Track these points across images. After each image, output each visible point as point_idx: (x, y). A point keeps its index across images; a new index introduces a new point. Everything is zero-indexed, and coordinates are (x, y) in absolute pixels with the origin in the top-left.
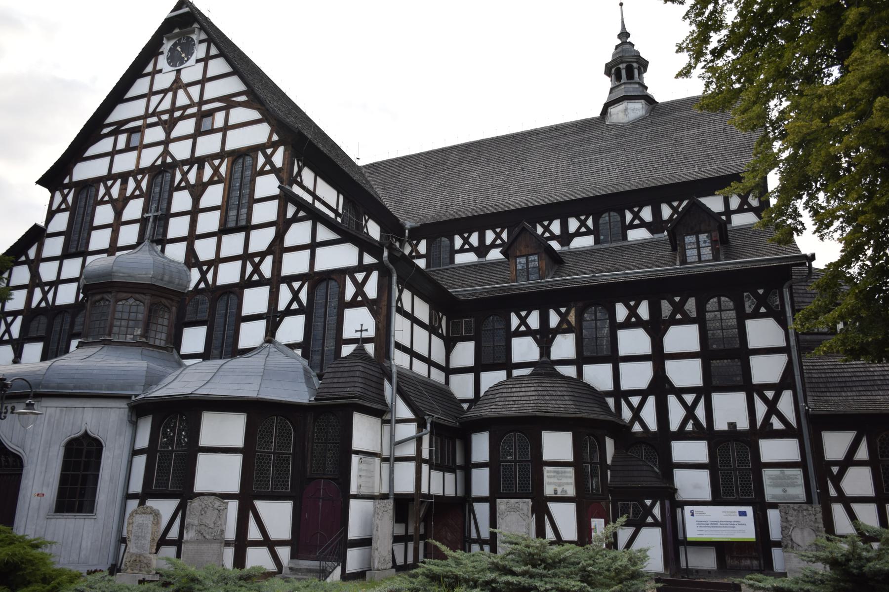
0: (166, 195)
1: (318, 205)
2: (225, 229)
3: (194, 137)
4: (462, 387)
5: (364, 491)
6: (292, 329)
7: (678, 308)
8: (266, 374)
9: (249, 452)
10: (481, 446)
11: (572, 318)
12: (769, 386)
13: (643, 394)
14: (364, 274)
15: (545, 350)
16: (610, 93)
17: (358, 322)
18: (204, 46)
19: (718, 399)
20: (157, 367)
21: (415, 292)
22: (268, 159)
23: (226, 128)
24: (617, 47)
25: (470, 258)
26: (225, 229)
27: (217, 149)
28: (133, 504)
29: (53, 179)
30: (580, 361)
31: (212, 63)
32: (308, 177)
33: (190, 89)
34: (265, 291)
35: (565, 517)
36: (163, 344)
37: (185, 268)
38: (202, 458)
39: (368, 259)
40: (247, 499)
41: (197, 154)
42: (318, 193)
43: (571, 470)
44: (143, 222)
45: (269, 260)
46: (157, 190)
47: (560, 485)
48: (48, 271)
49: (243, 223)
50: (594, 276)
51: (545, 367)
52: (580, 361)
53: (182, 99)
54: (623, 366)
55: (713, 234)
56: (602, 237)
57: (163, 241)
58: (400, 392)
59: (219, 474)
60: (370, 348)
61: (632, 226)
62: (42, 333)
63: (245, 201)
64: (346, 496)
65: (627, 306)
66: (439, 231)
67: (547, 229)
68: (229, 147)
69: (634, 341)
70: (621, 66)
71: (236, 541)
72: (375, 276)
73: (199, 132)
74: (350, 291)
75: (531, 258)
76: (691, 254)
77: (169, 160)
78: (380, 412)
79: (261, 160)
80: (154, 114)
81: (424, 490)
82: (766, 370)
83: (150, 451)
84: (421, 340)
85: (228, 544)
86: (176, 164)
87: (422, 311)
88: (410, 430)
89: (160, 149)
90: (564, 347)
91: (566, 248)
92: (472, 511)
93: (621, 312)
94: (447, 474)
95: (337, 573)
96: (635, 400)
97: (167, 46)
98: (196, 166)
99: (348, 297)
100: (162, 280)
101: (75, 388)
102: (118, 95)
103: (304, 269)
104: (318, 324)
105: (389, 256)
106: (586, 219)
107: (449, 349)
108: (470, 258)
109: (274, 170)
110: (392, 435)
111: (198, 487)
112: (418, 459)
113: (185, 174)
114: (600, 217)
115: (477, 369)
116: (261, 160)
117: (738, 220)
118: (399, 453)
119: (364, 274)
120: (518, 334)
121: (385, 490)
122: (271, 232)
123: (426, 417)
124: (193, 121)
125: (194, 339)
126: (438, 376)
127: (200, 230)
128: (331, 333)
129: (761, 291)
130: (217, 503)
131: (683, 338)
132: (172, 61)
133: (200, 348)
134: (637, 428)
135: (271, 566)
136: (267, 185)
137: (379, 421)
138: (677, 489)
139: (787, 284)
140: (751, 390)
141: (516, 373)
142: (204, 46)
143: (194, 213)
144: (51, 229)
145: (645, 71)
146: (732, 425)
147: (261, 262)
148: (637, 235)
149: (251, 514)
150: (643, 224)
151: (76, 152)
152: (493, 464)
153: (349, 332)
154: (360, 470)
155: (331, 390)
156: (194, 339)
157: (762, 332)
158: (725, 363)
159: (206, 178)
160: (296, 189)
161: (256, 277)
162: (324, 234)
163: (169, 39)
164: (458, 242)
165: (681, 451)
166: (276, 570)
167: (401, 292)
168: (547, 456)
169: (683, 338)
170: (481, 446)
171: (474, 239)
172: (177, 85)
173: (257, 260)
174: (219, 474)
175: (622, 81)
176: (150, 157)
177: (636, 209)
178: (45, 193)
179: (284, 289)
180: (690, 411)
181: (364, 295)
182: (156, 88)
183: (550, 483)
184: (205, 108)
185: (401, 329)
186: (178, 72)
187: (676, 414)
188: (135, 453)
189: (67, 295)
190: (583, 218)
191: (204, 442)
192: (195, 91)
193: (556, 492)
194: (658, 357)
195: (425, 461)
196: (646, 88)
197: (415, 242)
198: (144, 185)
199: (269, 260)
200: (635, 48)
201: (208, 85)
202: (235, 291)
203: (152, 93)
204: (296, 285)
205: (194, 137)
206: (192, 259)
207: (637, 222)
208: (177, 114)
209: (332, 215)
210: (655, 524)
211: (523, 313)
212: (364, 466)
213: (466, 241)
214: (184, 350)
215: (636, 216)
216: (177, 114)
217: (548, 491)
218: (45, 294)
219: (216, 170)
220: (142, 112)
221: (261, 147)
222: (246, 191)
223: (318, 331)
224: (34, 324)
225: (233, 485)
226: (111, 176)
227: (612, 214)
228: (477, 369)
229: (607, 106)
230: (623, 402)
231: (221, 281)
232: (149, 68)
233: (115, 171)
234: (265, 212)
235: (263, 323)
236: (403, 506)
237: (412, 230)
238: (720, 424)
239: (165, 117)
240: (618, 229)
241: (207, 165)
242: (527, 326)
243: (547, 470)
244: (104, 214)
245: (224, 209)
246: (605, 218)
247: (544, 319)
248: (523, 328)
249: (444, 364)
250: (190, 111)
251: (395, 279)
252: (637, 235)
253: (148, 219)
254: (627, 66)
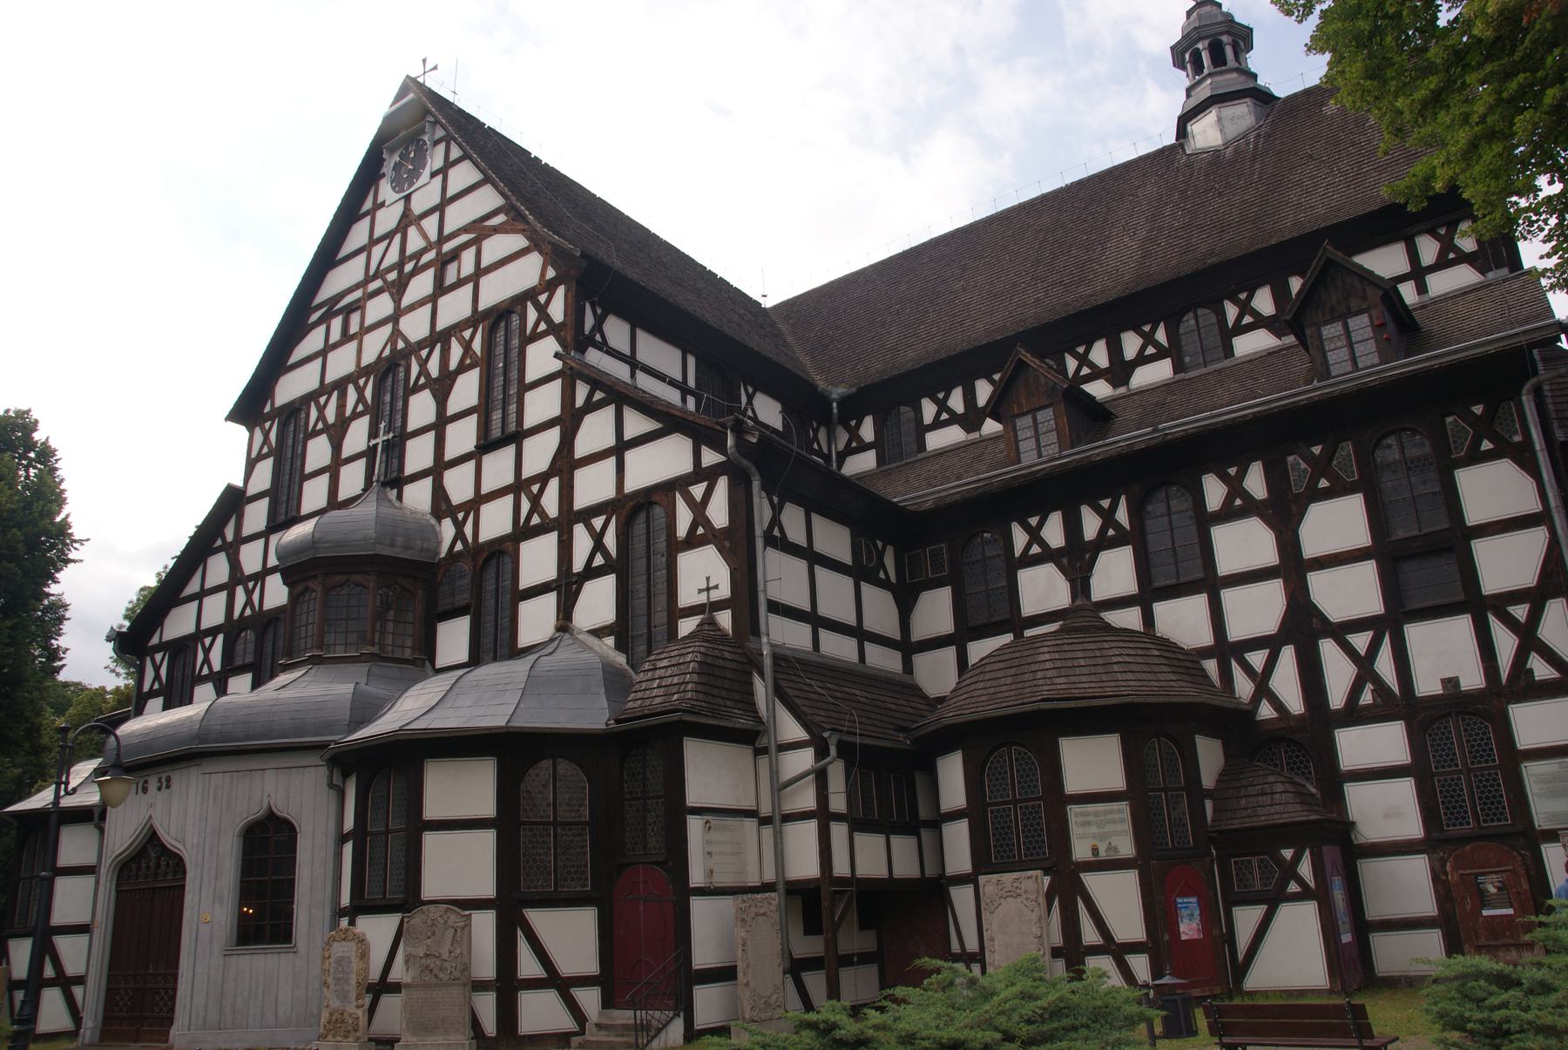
0: (400, 403)
1: (645, 382)
2: (487, 445)
3: (433, 299)
4: (937, 673)
5: (723, 879)
6: (598, 602)
7: (1321, 467)
8: (533, 683)
9: (508, 823)
10: (952, 777)
11: (1122, 515)
12: (1515, 596)
13: (1271, 644)
14: (705, 484)
15: (1080, 585)
16: (1188, 96)
17: (702, 574)
18: (441, 148)
19: (1418, 635)
20: (376, 690)
21: (813, 506)
22: (542, 311)
23: (480, 272)
24: (1189, 14)
25: (953, 435)
26: (487, 445)
27: (465, 311)
28: (344, 922)
29: (249, 409)
30: (1148, 594)
31: (453, 173)
32: (617, 331)
33: (424, 223)
34: (550, 541)
35: (1119, 901)
36: (408, 654)
37: (433, 521)
38: (430, 840)
39: (710, 457)
40: (510, 906)
41: (441, 324)
42: (642, 356)
43: (1123, 808)
44: (369, 453)
45: (554, 484)
46: (388, 398)
47: (1102, 837)
48: (251, 558)
49: (512, 427)
50: (1155, 430)
51: (1083, 616)
52: (1148, 594)
53: (415, 242)
54: (1229, 596)
55: (1374, 313)
56: (1187, 359)
57: (397, 481)
58: (779, 692)
59: (460, 866)
60: (725, 619)
61: (1240, 329)
62: (249, 659)
63: (513, 391)
64: (684, 892)
65: (1224, 478)
66: (892, 398)
67: (1083, 360)
68: (483, 305)
69: (1243, 544)
70: (1200, 46)
71: (497, 980)
72: (722, 485)
73: (441, 289)
74: (684, 518)
75: (1041, 416)
76: (1337, 358)
77: (401, 345)
78: (751, 737)
79: (532, 315)
80: (375, 277)
81: (841, 868)
82: (1506, 564)
83: (359, 835)
84: (836, 595)
85: (480, 986)
86: (413, 349)
87: (834, 540)
88: (804, 760)
89: (387, 330)
90: (1115, 573)
91: (1122, 390)
92: (946, 902)
93: (1214, 492)
94: (896, 841)
95: (676, 1030)
96: (1257, 659)
97: (391, 161)
98: (439, 346)
99: (682, 530)
100: (392, 545)
101: (247, 738)
102: (327, 257)
103: (607, 492)
104: (639, 584)
105: (737, 445)
106: (1154, 330)
107: (906, 607)
108: (953, 435)
109: (554, 329)
110: (774, 772)
111: (430, 890)
112: (823, 815)
113: (423, 364)
114: (1180, 321)
115: (959, 639)
116: (532, 315)
117: (1442, 283)
118: (790, 806)
119: (705, 484)
120: (1028, 561)
121: (770, 876)
122: (553, 437)
123: (826, 735)
124: (430, 273)
125: (454, 639)
126: (883, 660)
127: (450, 453)
128: (661, 602)
129: (1478, 409)
130: (454, 919)
131: (1336, 523)
132: (397, 185)
133: (463, 657)
134: (1266, 711)
135: (566, 1023)
136: (542, 357)
137: (746, 752)
138: (1353, 823)
139: (1528, 386)
140: (1481, 608)
141: (1028, 633)
142: (441, 148)
143: (440, 426)
144: (252, 490)
145: (1250, 47)
146: (1451, 683)
147: (541, 491)
148: (1250, 344)
149: (520, 933)
150: (1260, 322)
151: (276, 361)
152: (975, 812)
153: (688, 595)
154: (708, 842)
155: (648, 702)
156: (454, 639)
157: (1491, 489)
158: (1425, 562)
159: (453, 365)
160: (594, 357)
161: (536, 520)
162: (636, 423)
163: (392, 151)
164: (929, 410)
165: (1363, 745)
166: (577, 1029)
167: (777, 510)
168: (1072, 785)
169: (1336, 523)
170: (952, 777)
171: (956, 401)
172: (408, 220)
173: (535, 488)
174: (460, 866)
175: (1206, 71)
176: (375, 346)
177: (1243, 296)
178: (240, 433)
179: (579, 531)
180: (1364, 665)
181: (707, 523)
182: (378, 233)
183: (1083, 837)
184: (447, 247)
185: (783, 577)
186: (408, 198)
187: (1338, 673)
188: (342, 839)
190: (1147, 328)
191: (431, 811)
192: (430, 225)
193: (1095, 851)
194: (1293, 567)
195: (839, 817)
196: (1255, 76)
197: (853, 423)
198: (368, 393)
199: (554, 484)
200: (1224, 9)
201: (451, 211)
202: (504, 551)
203: (373, 242)
204: (598, 522)
205: (433, 299)
206: (441, 504)
207: (1247, 319)
208: (409, 267)
209: (672, 396)
210: (1305, 895)
211: (1034, 521)
212: (714, 836)
213: (942, 406)
214: (440, 663)
215: (1245, 308)
216: (409, 267)
217: (1081, 851)
218: (249, 593)
220: (360, 276)
221: (530, 295)
222: (514, 374)
223: (639, 603)
224: (239, 648)
225: (485, 885)
226: (324, 389)
227: (1200, 312)
228: (959, 639)
229: (1184, 121)
230: (1234, 664)
231: (484, 537)
232: (368, 205)
233: (329, 378)
234: (542, 404)
235: (551, 599)
236: (809, 901)
237: (844, 402)
238: (1427, 684)
239: (392, 276)
240: (1214, 339)
242: (1043, 544)
243: (1074, 811)
244: (318, 452)
245: (483, 410)
246: (1189, 322)
247: (1073, 527)
248: (1035, 549)
249: (897, 635)
250: (426, 258)
251: (756, 485)
252: (1250, 344)
253: (376, 446)
254: (1212, 46)
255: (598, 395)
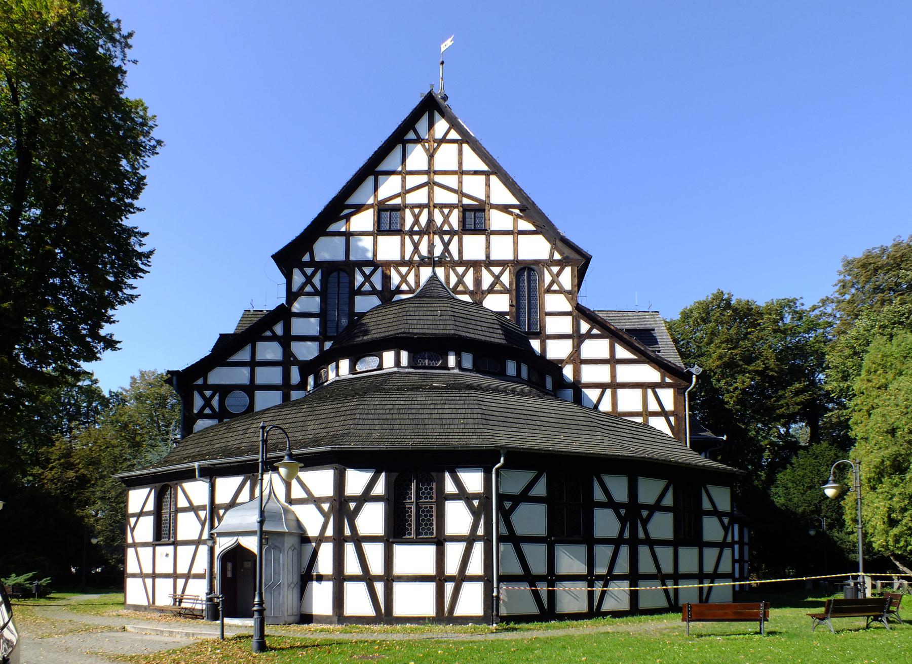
162: (622, 352)
219: (497, 278)
241: (484, 272)
255: (595, 331)
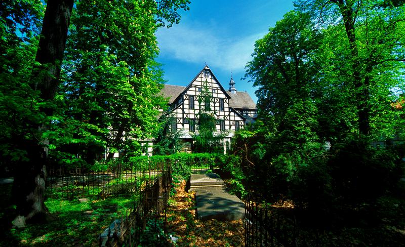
113: (212, 100)
189: (192, 116)
202: (224, 121)
226: (196, 95)
234: (226, 109)
244: (196, 103)
